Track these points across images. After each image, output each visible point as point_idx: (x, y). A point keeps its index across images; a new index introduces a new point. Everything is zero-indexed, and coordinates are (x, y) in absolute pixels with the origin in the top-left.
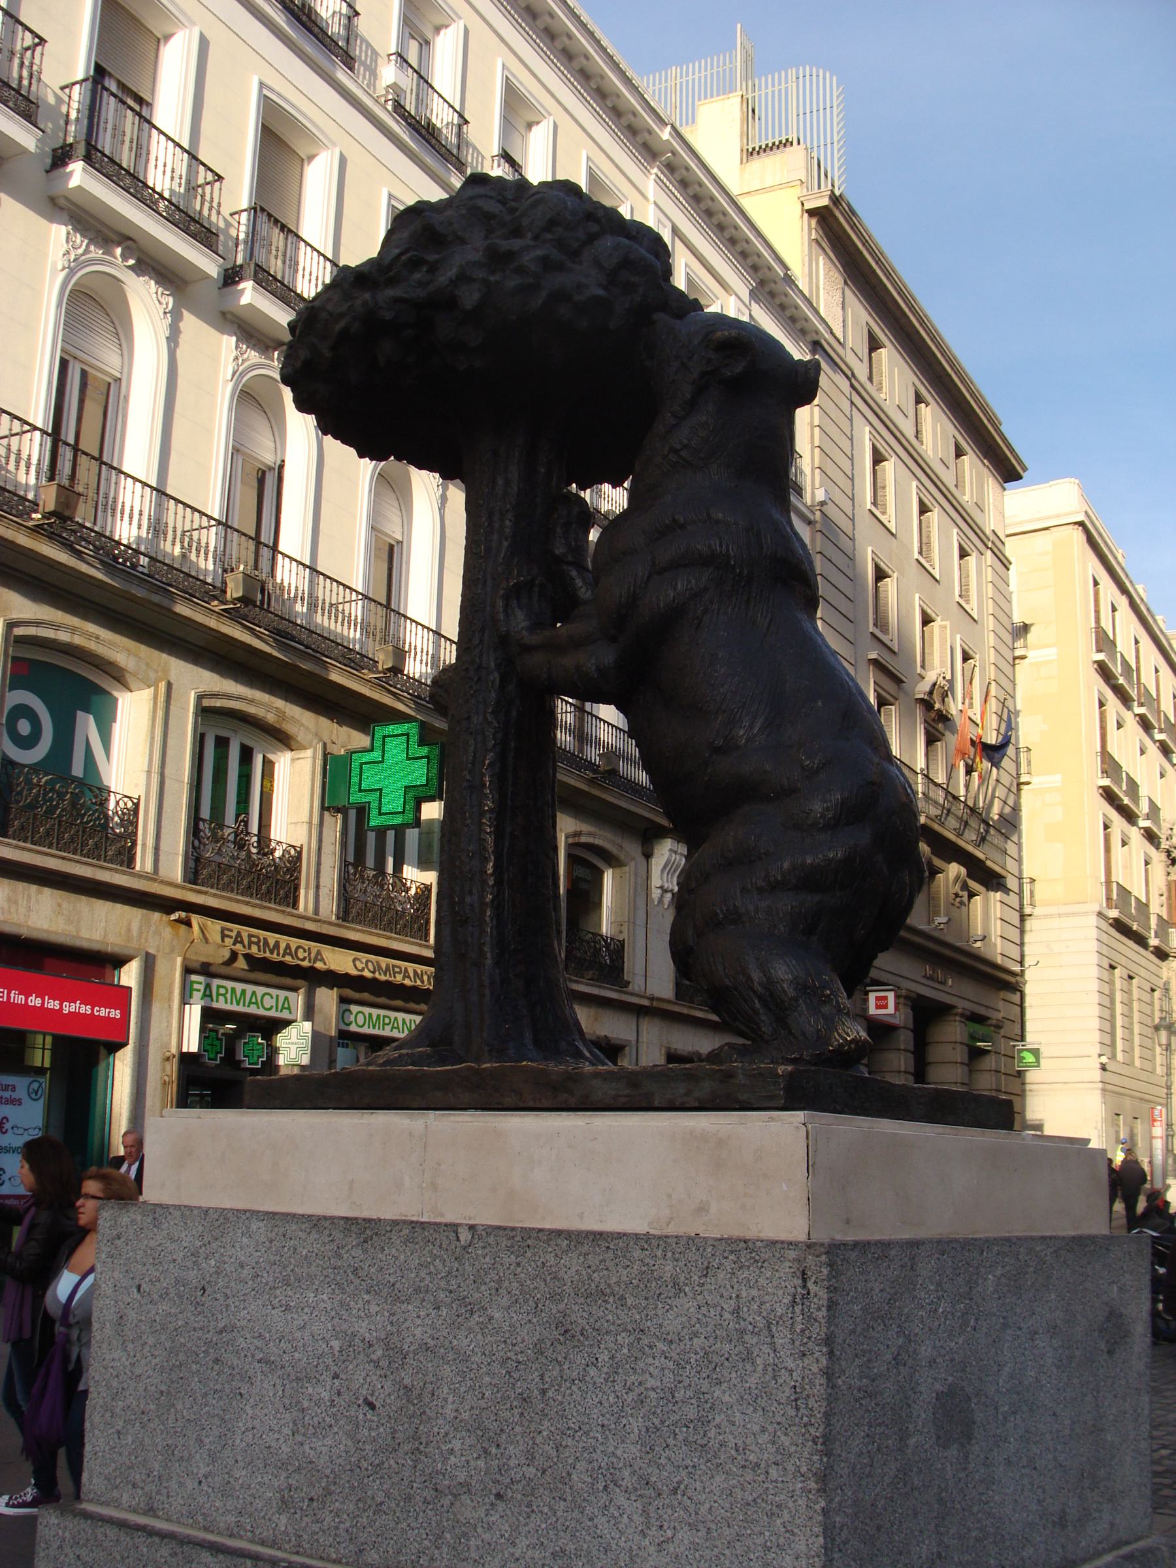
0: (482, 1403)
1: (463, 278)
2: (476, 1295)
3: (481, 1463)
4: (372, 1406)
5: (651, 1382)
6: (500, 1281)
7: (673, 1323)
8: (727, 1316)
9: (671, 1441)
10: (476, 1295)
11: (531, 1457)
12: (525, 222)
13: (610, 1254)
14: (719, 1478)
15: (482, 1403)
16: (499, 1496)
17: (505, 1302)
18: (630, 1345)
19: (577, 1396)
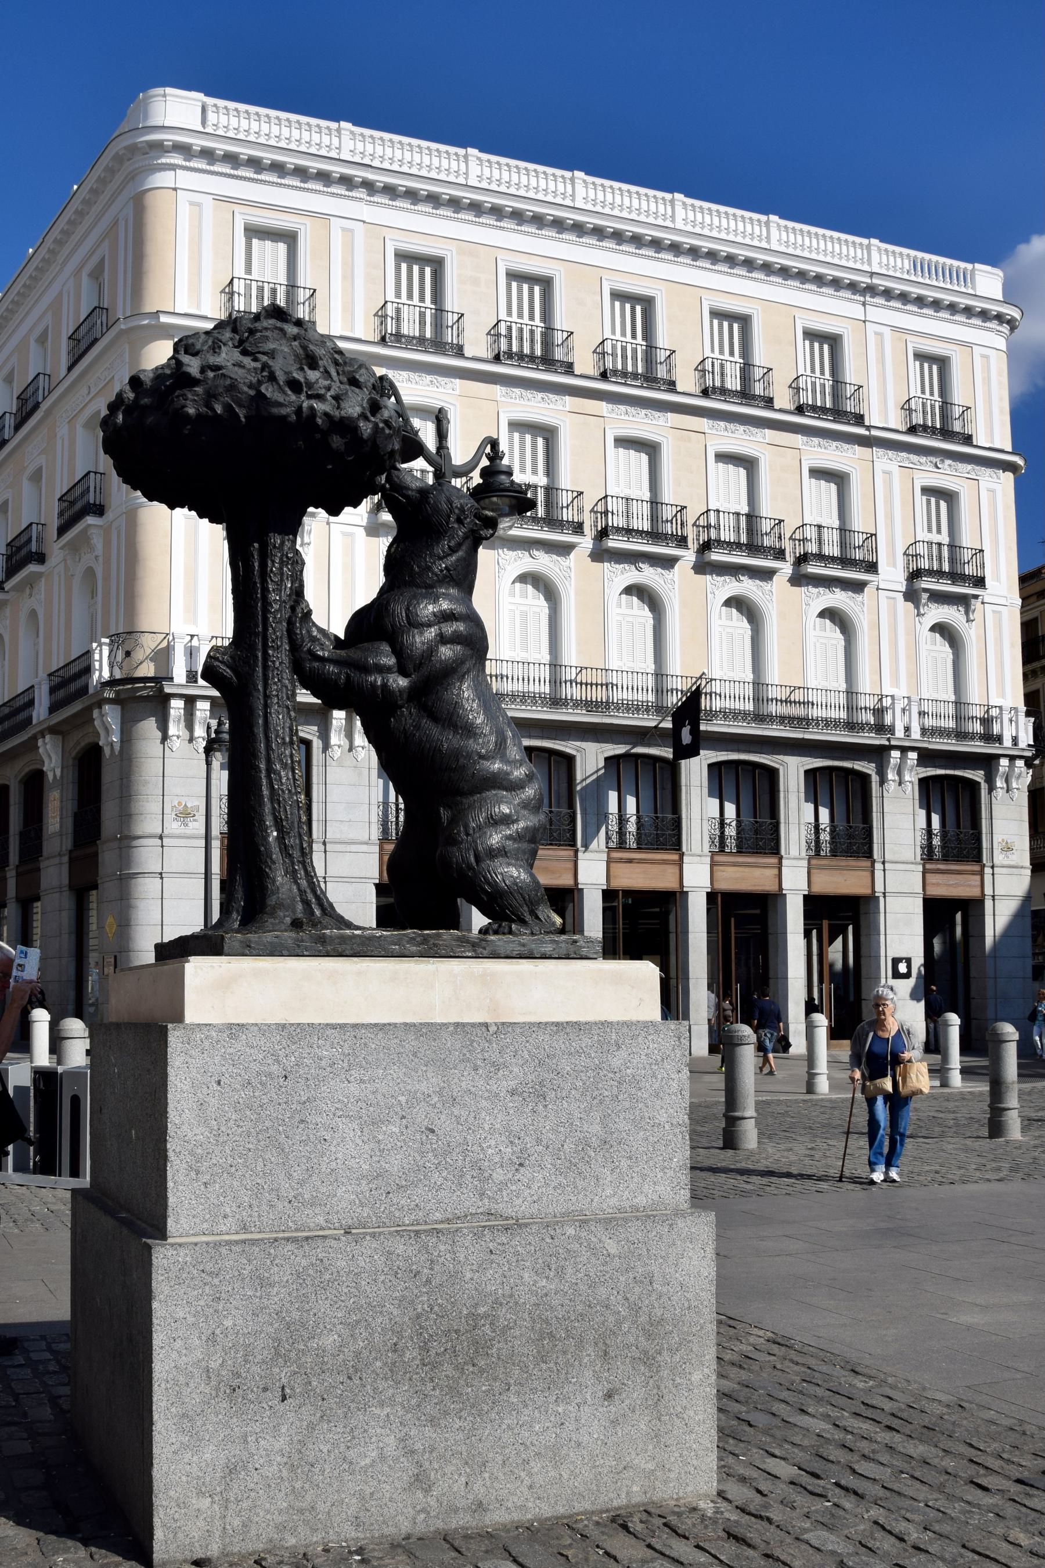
0: (508, 1118)
1: (363, 416)
2: (501, 1060)
3: (509, 1150)
4: (432, 1131)
5: (606, 1093)
6: (516, 1051)
7: (616, 1063)
8: (643, 1057)
9: (617, 1120)
10: (501, 1060)
11: (539, 1141)
12: (362, 380)
13: (582, 1032)
14: (642, 1133)
15: (508, 1118)
16: (521, 1165)
17: (521, 1062)
18: (594, 1077)
19: (565, 1105)
